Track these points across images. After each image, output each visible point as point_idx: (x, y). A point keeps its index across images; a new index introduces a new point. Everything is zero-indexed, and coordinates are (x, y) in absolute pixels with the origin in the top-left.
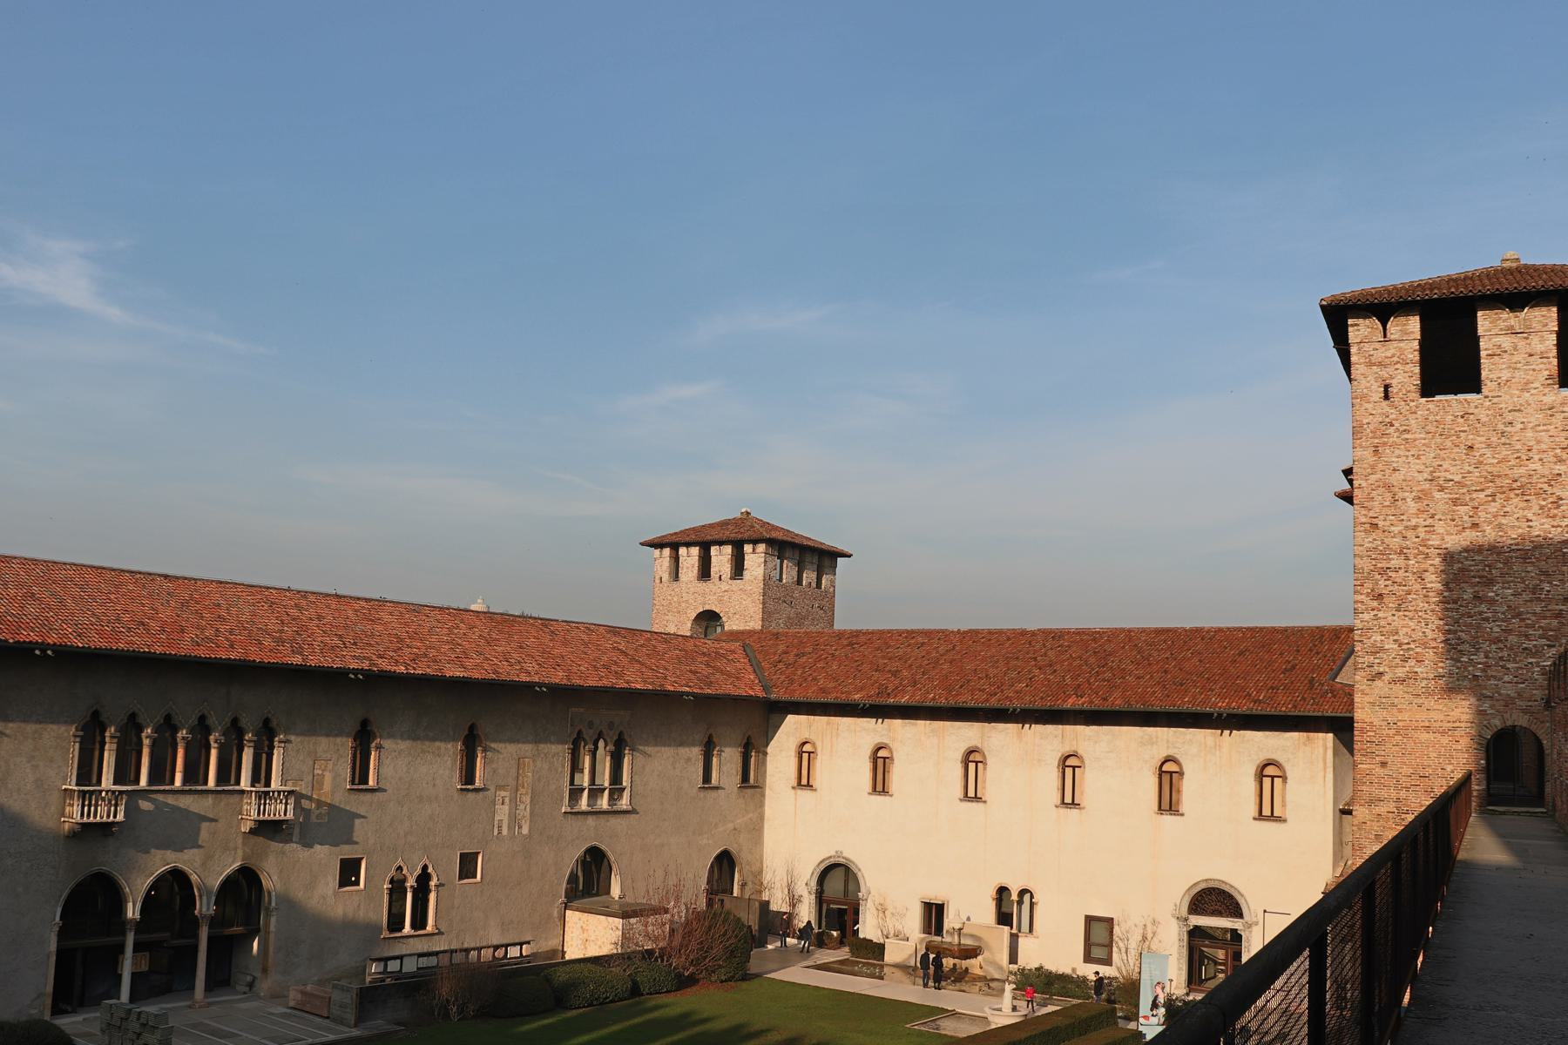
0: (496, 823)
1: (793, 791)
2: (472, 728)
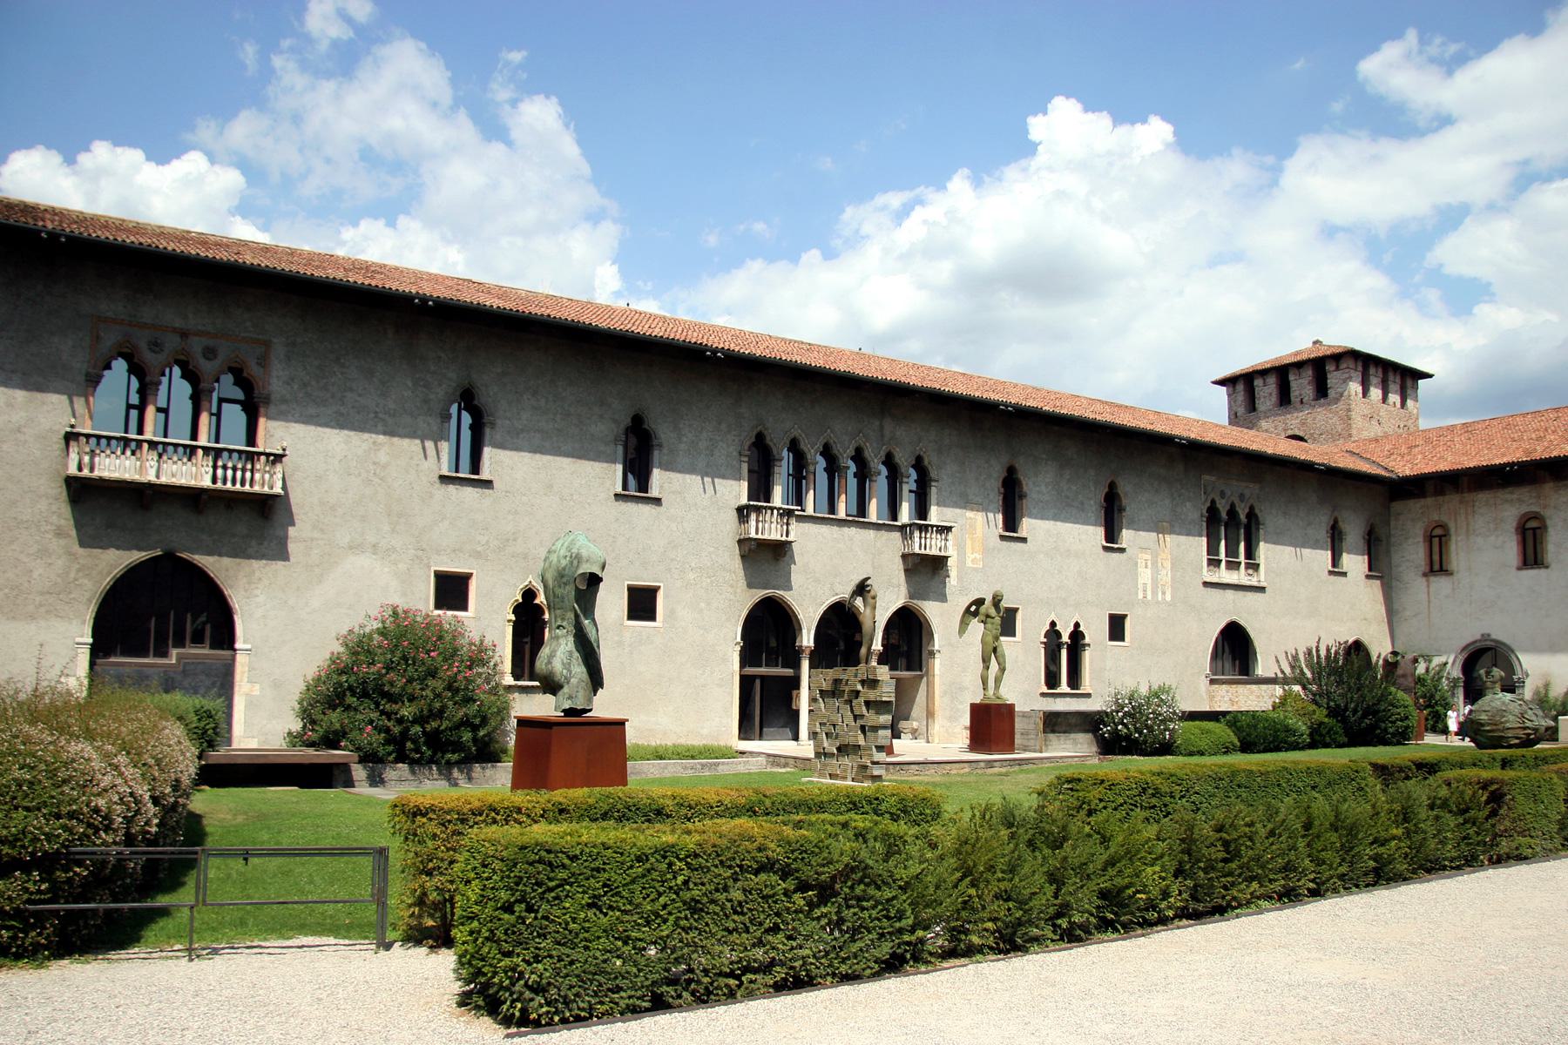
1: (1424, 579)
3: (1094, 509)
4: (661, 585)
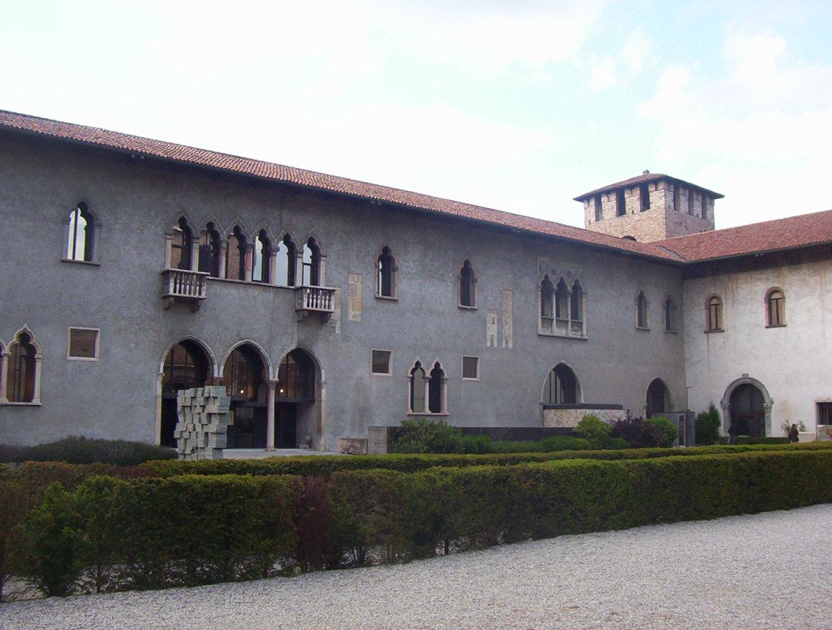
0: (488, 337)
2: (467, 263)
4: (99, 330)
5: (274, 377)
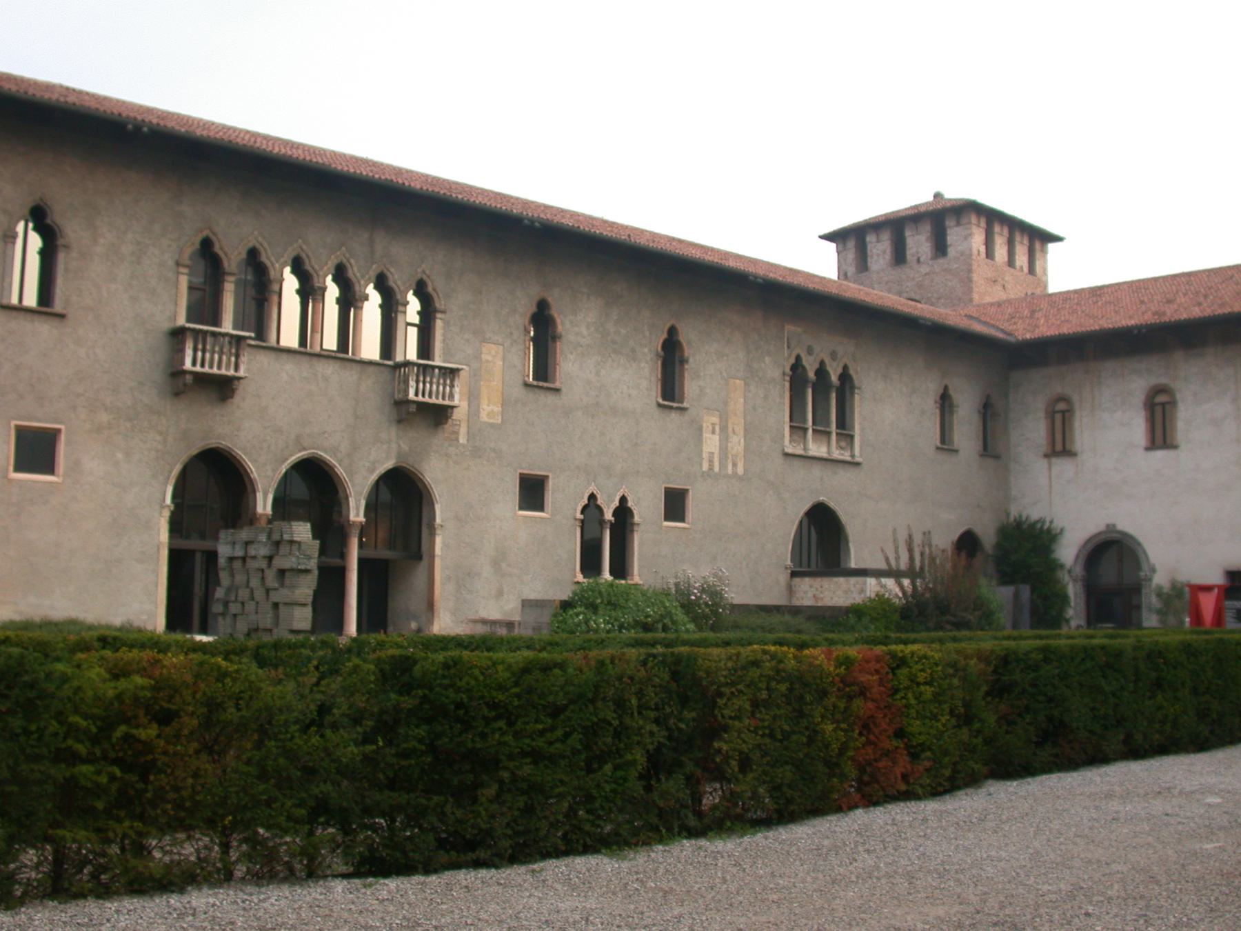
0: (705, 455)
1: (1043, 463)
2: (672, 331)
3: (648, 359)
5: (357, 515)
